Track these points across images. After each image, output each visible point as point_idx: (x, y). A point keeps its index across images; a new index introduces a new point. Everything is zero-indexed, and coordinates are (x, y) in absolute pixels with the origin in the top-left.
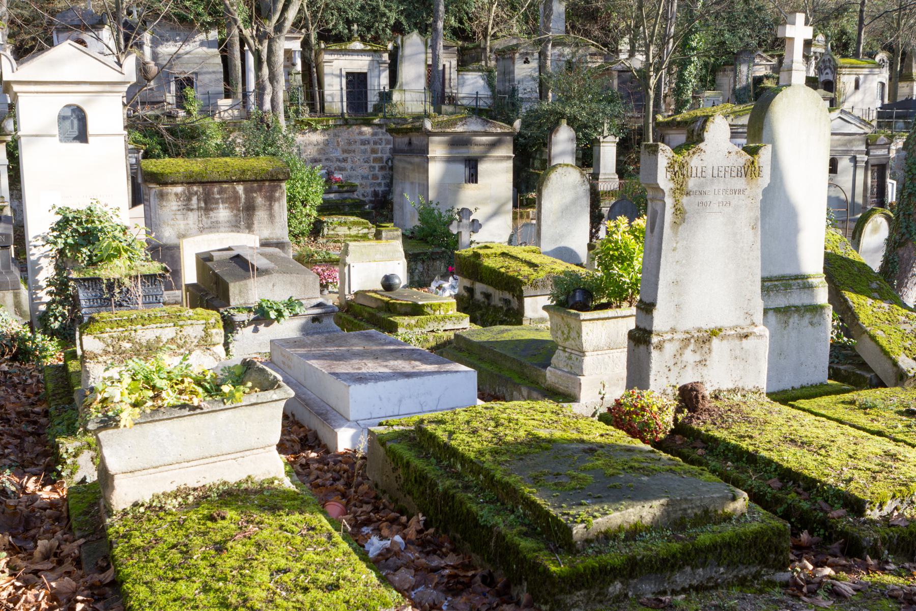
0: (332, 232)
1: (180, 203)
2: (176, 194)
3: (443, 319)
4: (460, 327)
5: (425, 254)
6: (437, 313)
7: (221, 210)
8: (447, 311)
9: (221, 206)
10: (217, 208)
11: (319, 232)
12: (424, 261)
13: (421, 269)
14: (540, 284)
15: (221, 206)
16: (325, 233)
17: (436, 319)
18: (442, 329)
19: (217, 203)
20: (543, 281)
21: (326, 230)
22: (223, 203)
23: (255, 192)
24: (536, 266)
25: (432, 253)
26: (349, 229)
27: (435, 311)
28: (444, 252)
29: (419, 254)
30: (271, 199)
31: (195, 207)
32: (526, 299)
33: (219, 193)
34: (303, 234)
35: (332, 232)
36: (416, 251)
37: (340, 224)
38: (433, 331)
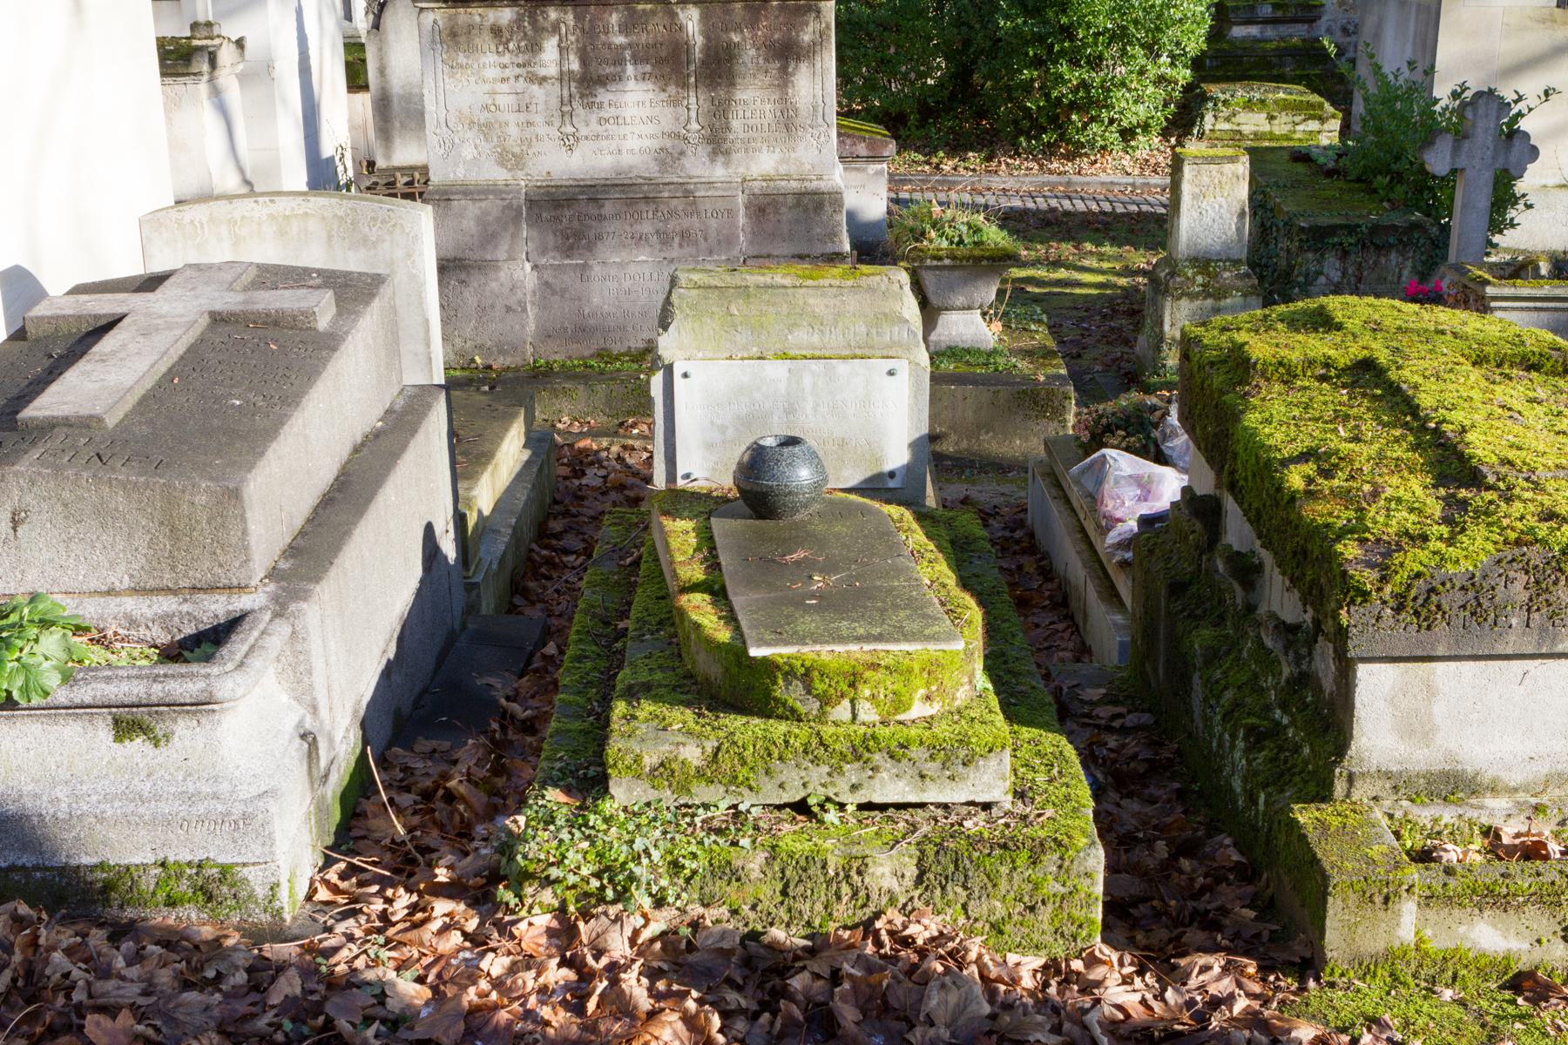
0: (1227, 126)
1: (506, 59)
2: (496, 31)
3: (861, 751)
4: (956, 794)
5: (1351, 229)
6: (842, 711)
7: (631, 84)
8: (900, 704)
9: (630, 69)
10: (619, 78)
11: (1193, 124)
14: (1451, 600)
15: (630, 69)
16: (1208, 127)
17: (819, 749)
18: (851, 801)
19: (619, 61)
20: (1471, 583)
21: (1209, 118)
22: (636, 60)
23: (738, 28)
24: (1474, 478)
25: (1375, 229)
26: (1271, 118)
27: (825, 701)
28: (1416, 226)
29: (1332, 230)
30: (786, 54)
31: (552, 71)
32: (1363, 670)
33: (625, 29)
34: (1146, 127)
35: (1227, 126)
36: (1324, 220)
37: (1249, 105)
38: (801, 807)
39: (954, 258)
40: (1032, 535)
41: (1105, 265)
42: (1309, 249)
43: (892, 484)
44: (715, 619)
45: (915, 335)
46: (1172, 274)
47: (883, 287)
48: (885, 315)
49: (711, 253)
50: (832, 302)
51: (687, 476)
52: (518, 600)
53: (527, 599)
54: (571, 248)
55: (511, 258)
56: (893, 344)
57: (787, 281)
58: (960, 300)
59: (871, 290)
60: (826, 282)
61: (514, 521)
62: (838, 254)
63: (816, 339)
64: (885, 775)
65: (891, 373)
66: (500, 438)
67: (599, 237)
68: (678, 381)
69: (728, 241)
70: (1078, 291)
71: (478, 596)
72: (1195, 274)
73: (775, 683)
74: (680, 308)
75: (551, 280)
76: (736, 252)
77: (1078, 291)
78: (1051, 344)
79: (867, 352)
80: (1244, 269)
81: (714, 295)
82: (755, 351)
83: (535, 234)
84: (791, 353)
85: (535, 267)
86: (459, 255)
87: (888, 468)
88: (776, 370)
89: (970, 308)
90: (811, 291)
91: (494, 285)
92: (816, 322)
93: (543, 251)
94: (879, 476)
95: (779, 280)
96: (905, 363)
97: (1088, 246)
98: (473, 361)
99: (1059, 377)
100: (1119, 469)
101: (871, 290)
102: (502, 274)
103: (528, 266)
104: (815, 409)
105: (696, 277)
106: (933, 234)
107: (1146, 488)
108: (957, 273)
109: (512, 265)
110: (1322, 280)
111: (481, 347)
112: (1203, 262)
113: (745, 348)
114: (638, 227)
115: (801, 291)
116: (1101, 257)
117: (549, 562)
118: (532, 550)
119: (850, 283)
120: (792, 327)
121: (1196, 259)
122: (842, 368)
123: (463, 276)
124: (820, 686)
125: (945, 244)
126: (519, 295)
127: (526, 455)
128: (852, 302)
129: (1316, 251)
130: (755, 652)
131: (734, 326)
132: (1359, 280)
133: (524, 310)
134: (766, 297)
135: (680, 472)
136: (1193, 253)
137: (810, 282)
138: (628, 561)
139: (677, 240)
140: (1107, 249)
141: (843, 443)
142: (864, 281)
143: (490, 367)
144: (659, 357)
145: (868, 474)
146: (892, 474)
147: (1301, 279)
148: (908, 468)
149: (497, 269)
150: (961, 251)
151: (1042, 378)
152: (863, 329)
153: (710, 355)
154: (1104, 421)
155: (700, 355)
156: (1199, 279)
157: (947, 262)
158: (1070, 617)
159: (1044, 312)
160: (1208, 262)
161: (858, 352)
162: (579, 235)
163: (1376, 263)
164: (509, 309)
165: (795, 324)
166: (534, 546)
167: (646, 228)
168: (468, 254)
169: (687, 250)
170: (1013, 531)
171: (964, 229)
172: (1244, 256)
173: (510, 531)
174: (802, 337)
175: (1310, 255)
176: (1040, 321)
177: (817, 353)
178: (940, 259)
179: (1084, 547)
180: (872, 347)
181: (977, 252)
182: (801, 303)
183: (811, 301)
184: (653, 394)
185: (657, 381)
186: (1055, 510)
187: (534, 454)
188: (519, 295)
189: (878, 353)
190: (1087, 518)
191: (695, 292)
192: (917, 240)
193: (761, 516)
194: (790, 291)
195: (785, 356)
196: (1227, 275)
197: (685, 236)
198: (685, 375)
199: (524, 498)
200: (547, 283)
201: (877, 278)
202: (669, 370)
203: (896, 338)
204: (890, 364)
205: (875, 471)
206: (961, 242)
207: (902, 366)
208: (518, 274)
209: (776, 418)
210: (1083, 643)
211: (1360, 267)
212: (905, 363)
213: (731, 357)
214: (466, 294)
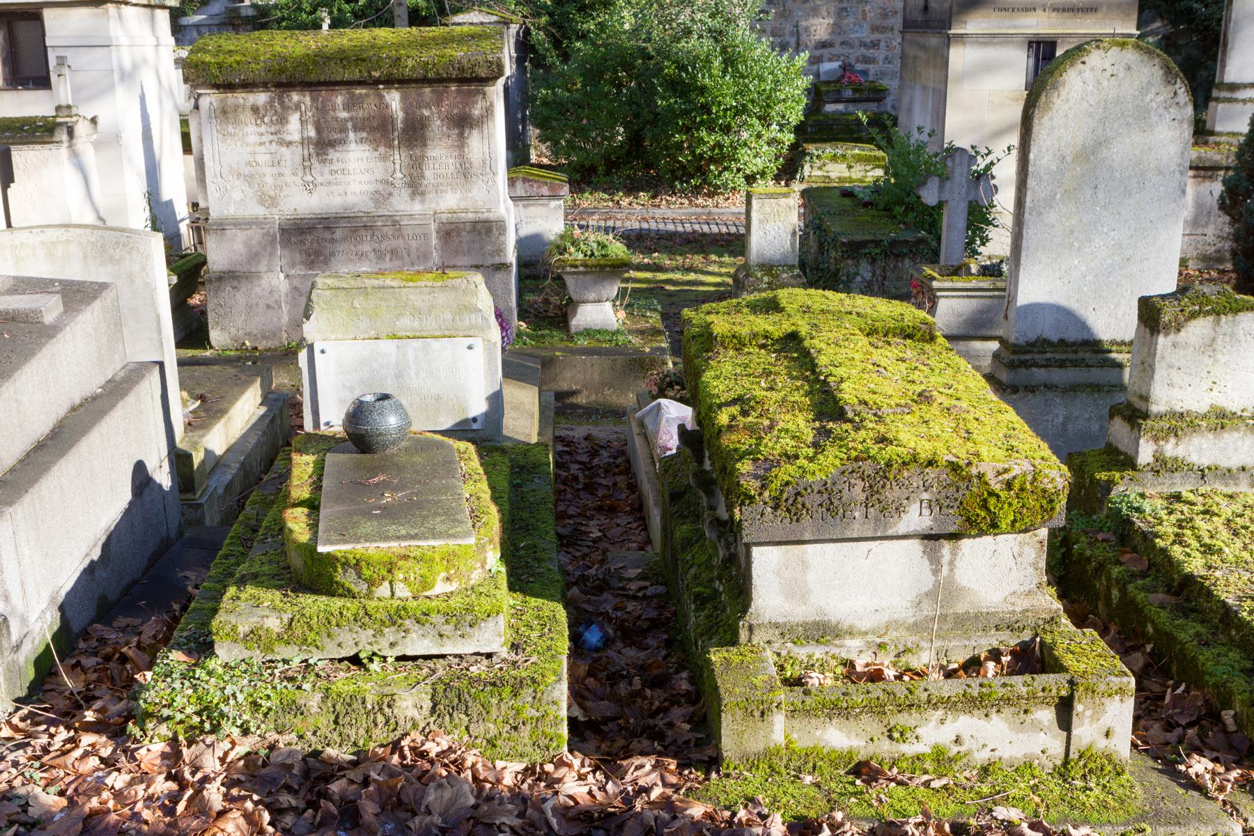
0: (819, 173)
1: (263, 129)
2: (255, 110)
3: (396, 618)
4: (467, 648)
5: (877, 243)
6: (383, 590)
7: (353, 146)
8: (426, 584)
9: (351, 135)
10: (343, 142)
11: (796, 172)
12: (874, 261)
13: (868, 276)
14: (812, 500)
15: (351, 135)
16: (806, 174)
17: (364, 618)
18: (391, 654)
19: (344, 130)
20: (825, 489)
21: (807, 167)
22: (356, 129)
23: (428, 106)
24: (839, 414)
25: (893, 243)
26: (850, 167)
27: (371, 583)
28: (921, 241)
29: (864, 244)
30: (463, 123)
31: (296, 137)
32: (756, 551)
33: (347, 107)
34: (763, 174)
35: (819, 173)
36: (859, 237)
37: (834, 158)
38: (355, 660)
39: (586, 266)
40: (628, 461)
41: (723, 270)
42: (849, 257)
43: (475, 426)
44: (304, 525)
46: (747, 276)
49: (413, 264)
50: (428, 297)
51: (327, 424)
54: (313, 262)
55: (270, 270)
56: (471, 327)
57: (395, 284)
58: (592, 296)
59: (454, 288)
60: (423, 284)
61: (242, 458)
62: (503, 264)
63: (416, 324)
64: (414, 635)
65: (470, 348)
67: (332, 254)
68: (318, 356)
69: (425, 256)
70: (701, 288)
71: (203, 513)
72: (763, 276)
73: (336, 571)
75: (298, 285)
76: (430, 264)
77: (701, 288)
78: (660, 326)
80: (797, 271)
81: (342, 294)
83: (286, 253)
84: (399, 334)
85: (287, 276)
86: (233, 269)
87: (471, 415)
88: (388, 346)
89: (599, 301)
91: (258, 290)
92: (417, 313)
93: (293, 265)
94: (465, 421)
95: (388, 282)
96: (479, 340)
97: (713, 257)
98: (244, 344)
99: (663, 349)
101: (454, 288)
102: (263, 282)
103: (282, 276)
104: (417, 374)
105: (329, 281)
106: (572, 249)
108: (589, 277)
109: (270, 275)
110: (859, 278)
111: (249, 334)
112: (768, 267)
113: (366, 332)
114: (360, 247)
115: (405, 290)
116: (721, 264)
119: (439, 284)
120: (399, 316)
121: (763, 265)
122: (435, 344)
123: (235, 283)
124: (367, 573)
125: (581, 256)
126: (276, 296)
127: (263, 410)
128: (442, 298)
129: (853, 258)
130: (321, 549)
131: (357, 316)
132: (884, 278)
133: (280, 307)
134: (379, 295)
135: (322, 421)
136: (761, 261)
137: (411, 284)
139: (388, 256)
140: (726, 259)
141: (438, 398)
142: (449, 283)
143: (256, 348)
145: (458, 420)
146: (475, 420)
147: (844, 278)
149: (260, 278)
150: (592, 261)
151: (648, 350)
152: (450, 316)
154: (668, 379)
156: (766, 279)
157: (581, 269)
159: (660, 302)
160: (772, 267)
161: (447, 333)
162: (318, 253)
163: (895, 267)
164: (269, 307)
165: (401, 314)
167: (366, 248)
168: (239, 268)
169: (397, 263)
170: (616, 458)
171: (595, 245)
172: (796, 263)
174: (406, 323)
175: (850, 262)
176: (655, 310)
177: (418, 334)
178: (576, 267)
181: (602, 262)
183: (412, 297)
188: (276, 296)
192: (561, 254)
193: (363, 452)
195: (394, 337)
196: (785, 276)
197: (394, 253)
198: (323, 352)
200: (296, 288)
201: (459, 280)
202: (311, 348)
203: (473, 322)
204: (469, 341)
205: (463, 417)
206: (593, 254)
207: (478, 342)
208: (275, 282)
210: (648, 537)
211: (884, 269)
212: (479, 340)
214: (238, 296)
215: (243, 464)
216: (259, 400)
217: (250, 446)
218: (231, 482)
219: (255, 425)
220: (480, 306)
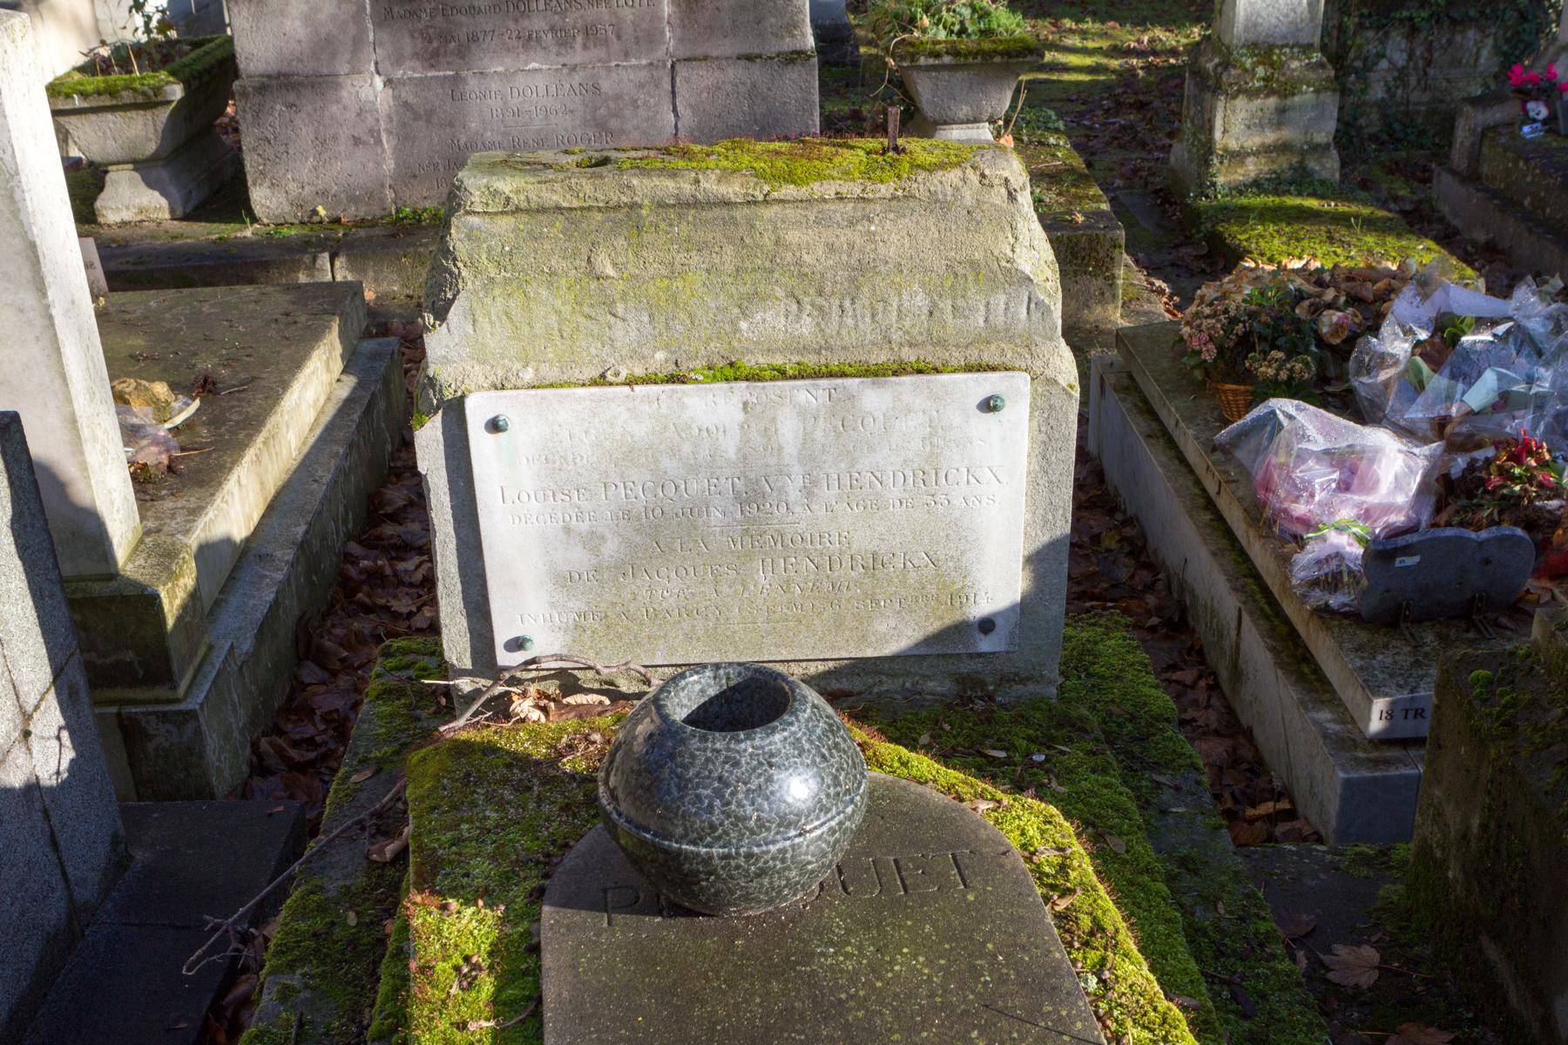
12: (1413, 30)
13: (1400, 59)
39: (955, 52)
41: (1090, 44)
42: (1371, 27)
43: (985, 645)
45: (1047, 311)
46: (1226, 65)
47: (968, 200)
48: (974, 265)
49: (626, 55)
50: (844, 237)
51: (517, 644)
52: (310, 673)
53: (324, 668)
54: (436, 53)
55: (355, 71)
56: (992, 333)
57: (733, 190)
58: (964, 111)
59: (939, 205)
60: (829, 189)
61: (301, 530)
62: (800, 53)
63: (806, 327)
65: (989, 405)
66: (297, 364)
67: (473, 38)
68: (480, 442)
69: (650, 38)
70: (1066, 77)
71: (198, 732)
72: (1255, 65)
74: (472, 264)
75: (411, 99)
76: (660, 53)
77: (1066, 77)
78: (1078, 162)
79: (931, 355)
80: (1316, 57)
82: (660, 359)
83: (386, 37)
84: (749, 362)
85: (389, 82)
86: (285, 69)
88: (713, 408)
89: (976, 120)
90: (790, 212)
91: (334, 108)
92: (808, 287)
93: (398, 61)
94: (960, 631)
95: (711, 185)
96: (1022, 381)
97: (1068, 23)
98: (315, 212)
99: (1100, 214)
100: (1304, 437)
101: (939, 205)
102: (344, 93)
103: (379, 82)
104: (808, 493)
105: (506, 185)
106: (926, 21)
107: (1351, 471)
108: (959, 75)
109: (357, 80)
110: (1384, 64)
111: (323, 194)
112: (1264, 49)
113: (636, 355)
114: (526, 23)
115: (769, 212)
116: (1084, 34)
117: (375, 578)
118: (349, 558)
119: (885, 190)
120: (746, 305)
121: (1255, 45)
122: (873, 398)
123: (292, 98)
125: (942, 35)
126: (370, 120)
127: (351, 381)
128: (895, 237)
129: (1379, 28)
132: (1429, 63)
133: (379, 141)
134: (682, 230)
135: (501, 636)
136: (1252, 37)
137: (789, 191)
138: (390, 849)
139: (579, 39)
140: (1089, 25)
141: (874, 564)
142: (922, 184)
143: (337, 221)
144: (432, 382)
145: (934, 626)
147: (1358, 64)
148: (1025, 607)
149: (337, 86)
150: (966, 44)
151: (1080, 219)
152: (921, 301)
153: (552, 374)
155: (529, 375)
156: (1260, 71)
157: (947, 59)
158: (1198, 654)
159: (1061, 115)
160: (1271, 48)
161: (908, 355)
162: (445, 37)
163: (1449, 42)
164: (357, 141)
165: (754, 296)
166: (355, 548)
167: (537, 24)
168: (296, 67)
169: (596, 53)
171: (967, 12)
172: (1317, 40)
173: (289, 555)
174: (773, 325)
175: (1370, 34)
176: (1057, 130)
177: (811, 361)
178: (938, 55)
179: (1224, 542)
180: (941, 343)
181: (986, 46)
182: (767, 241)
183: (793, 236)
184: (422, 467)
185: (429, 440)
186: (1154, 461)
187: (360, 386)
188: (370, 120)
189: (957, 358)
190: (1253, 525)
191: (505, 223)
192: (904, 30)
193: (676, 910)
194: (739, 214)
195: (731, 372)
196: (1295, 64)
197: (590, 33)
198: (495, 426)
199: (327, 477)
200: (406, 104)
201: (954, 175)
202: (455, 413)
203: (999, 319)
204: (987, 384)
205: (949, 620)
206: (963, 31)
207: (1017, 388)
208: (365, 93)
209: (717, 515)
210: (1231, 711)
211: (1430, 48)
212: (1022, 381)
213: (601, 381)
214: (298, 122)
215: (302, 546)
216: (338, 366)
217: (319, 490)
218: (275, 604)
219: (330, 428)
220: (1027, 269)
